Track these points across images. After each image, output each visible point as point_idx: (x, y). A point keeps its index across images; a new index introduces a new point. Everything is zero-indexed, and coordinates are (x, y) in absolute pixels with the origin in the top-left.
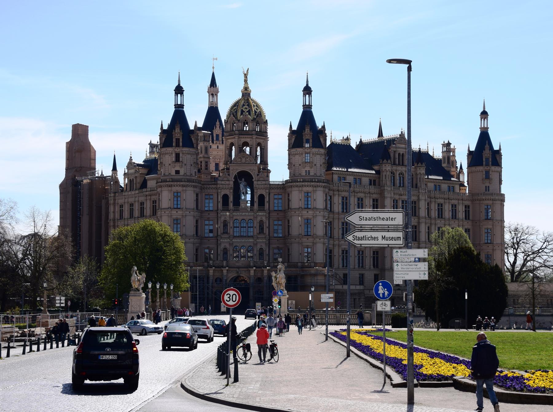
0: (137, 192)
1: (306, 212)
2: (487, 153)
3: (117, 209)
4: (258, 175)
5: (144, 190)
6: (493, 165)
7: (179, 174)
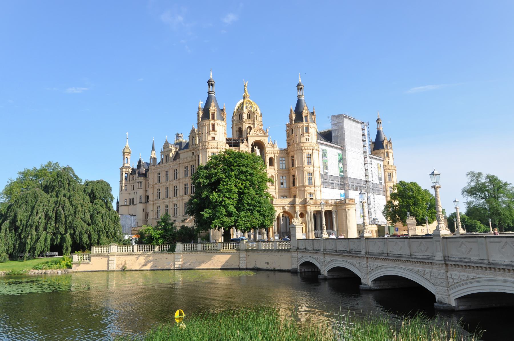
0: (172, 163)
3: (156, 176)
4: (269, 143)
5: (178, 160)
7: (214, 139)
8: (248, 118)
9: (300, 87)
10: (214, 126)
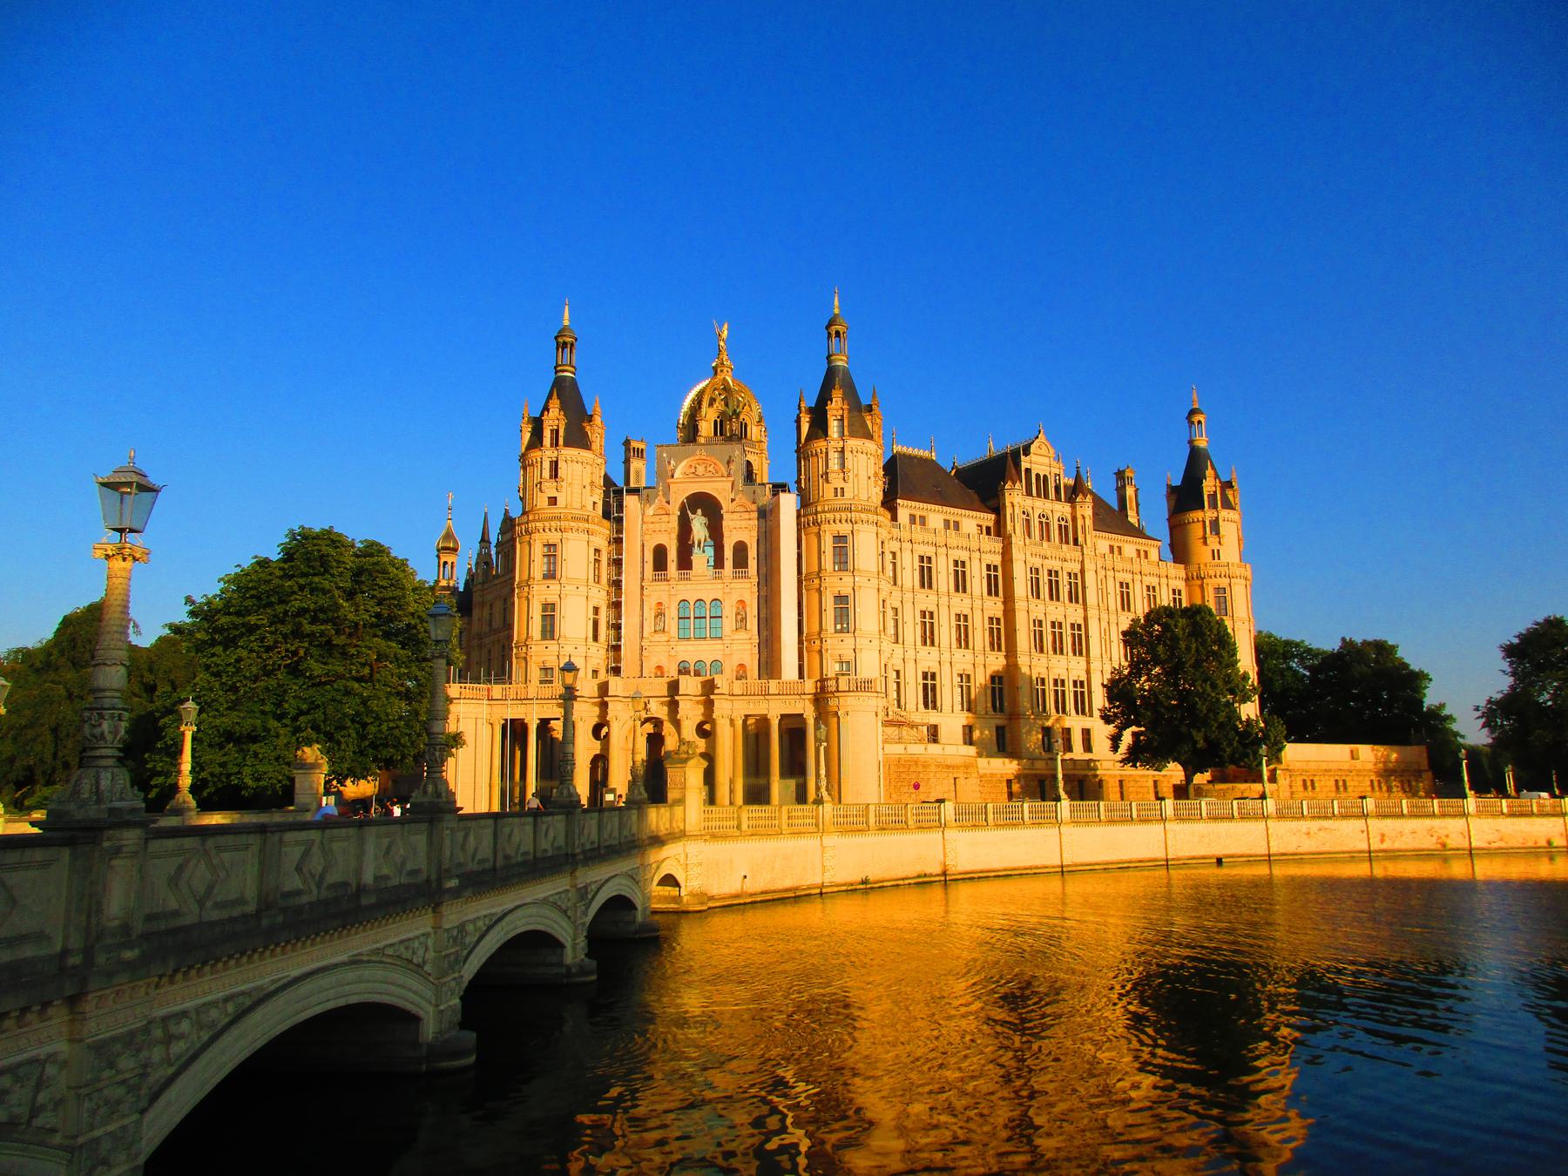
1: (836, 580)
2: (1209, 485)
6: (1223, 507)
8: (716, 434)
9: (834, 328)
10: (555, 466)
